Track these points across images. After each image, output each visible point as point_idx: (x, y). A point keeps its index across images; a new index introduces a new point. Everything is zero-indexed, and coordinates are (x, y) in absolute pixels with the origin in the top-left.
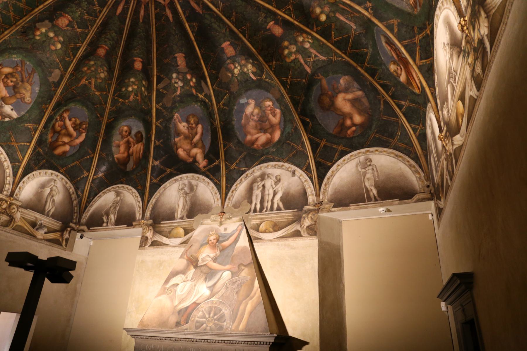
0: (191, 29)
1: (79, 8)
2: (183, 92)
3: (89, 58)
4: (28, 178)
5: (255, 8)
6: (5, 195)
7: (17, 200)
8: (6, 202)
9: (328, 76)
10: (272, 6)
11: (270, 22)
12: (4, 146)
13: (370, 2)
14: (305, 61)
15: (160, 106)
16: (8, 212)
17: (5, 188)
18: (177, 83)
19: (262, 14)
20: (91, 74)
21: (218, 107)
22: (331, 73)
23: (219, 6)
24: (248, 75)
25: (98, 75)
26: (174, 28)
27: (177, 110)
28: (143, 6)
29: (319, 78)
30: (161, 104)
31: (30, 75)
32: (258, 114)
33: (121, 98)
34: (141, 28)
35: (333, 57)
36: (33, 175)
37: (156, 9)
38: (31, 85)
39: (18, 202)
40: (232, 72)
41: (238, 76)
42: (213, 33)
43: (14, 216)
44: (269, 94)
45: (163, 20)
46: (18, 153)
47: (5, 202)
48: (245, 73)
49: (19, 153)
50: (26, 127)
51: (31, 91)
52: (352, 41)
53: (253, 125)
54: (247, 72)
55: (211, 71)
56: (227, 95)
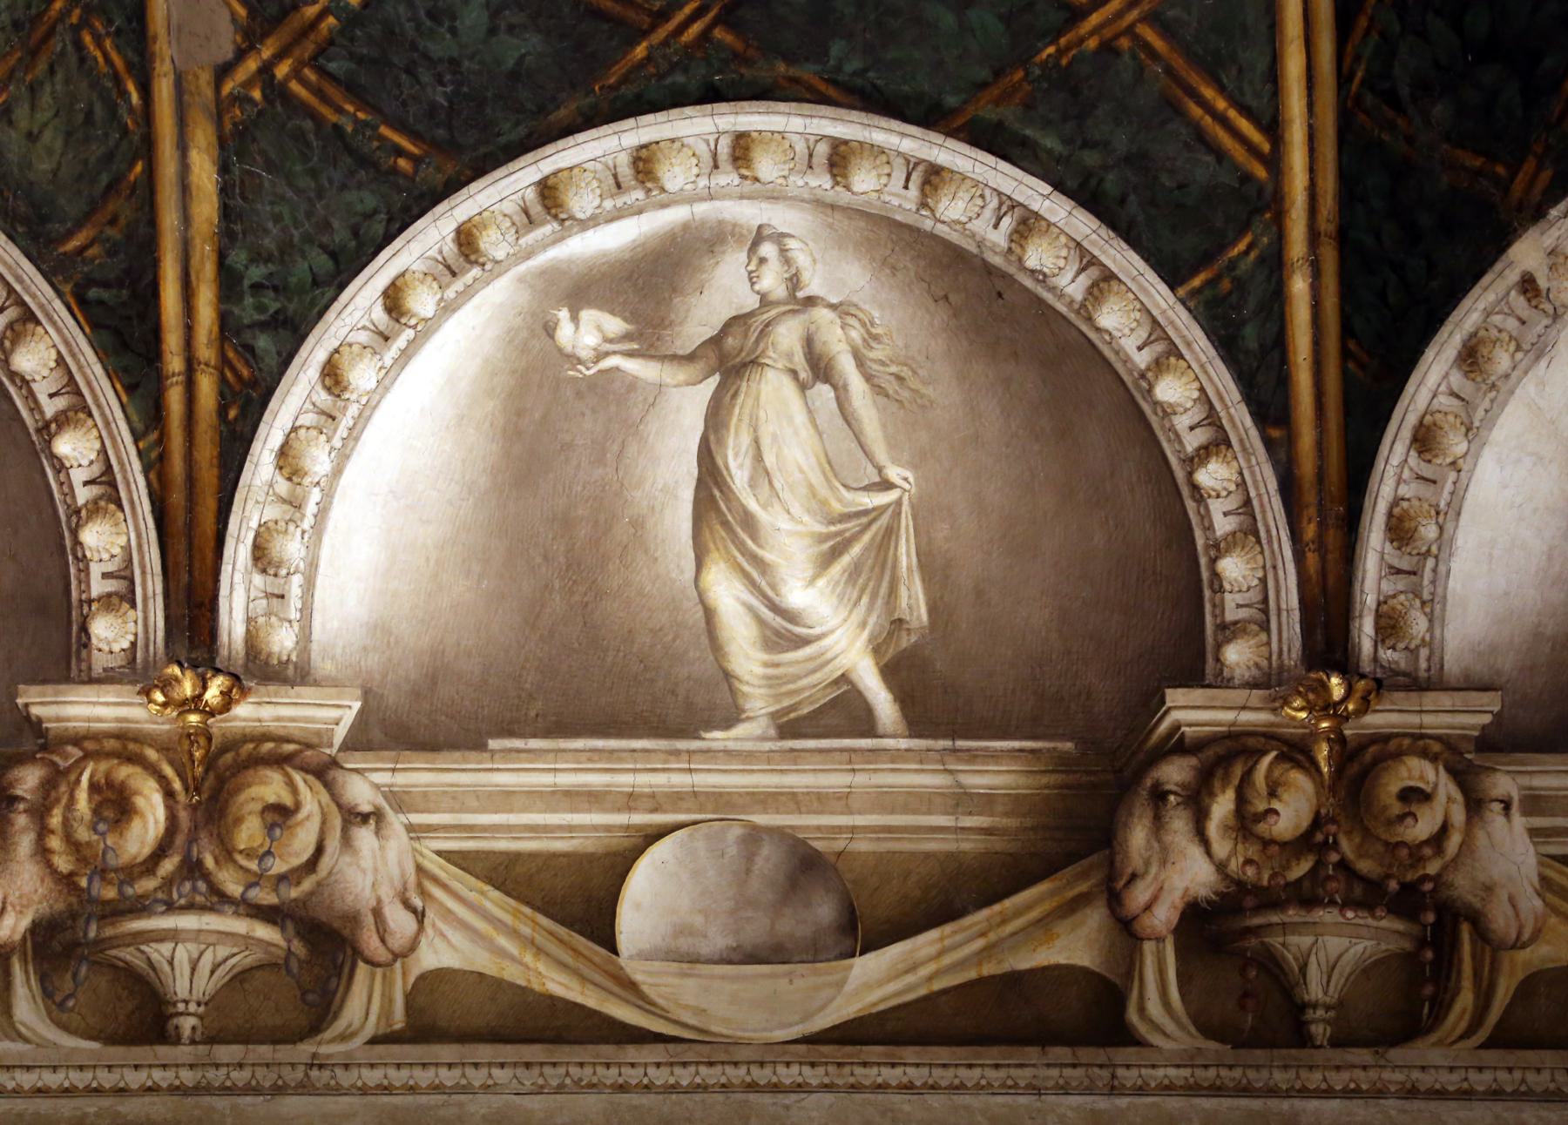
4: (1471, 357)
6: (1252, 685)
7: (1415, 684)
8: (1296, 751)
12: (1009, 113)
16: (1365, 866)
17: (1219, 607)
36: (1528, 285)
39: (1446, 700)
43: (1462, 886)
46: (1196, 111)
47: (1281, 758)
49: (1208, 93)
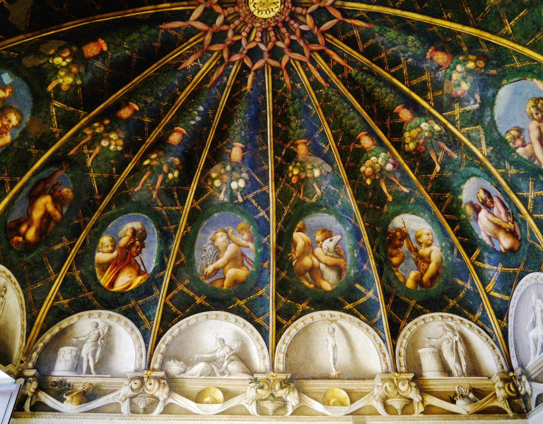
5: (160, 95)
9: (67, 174)
11: (137, 104)
13: (191, 229)
14: (84, 144)
22: (71, 175)
29: (64, 165)
35: (94, 173)
40: (58, 54)
52: (124, 193)
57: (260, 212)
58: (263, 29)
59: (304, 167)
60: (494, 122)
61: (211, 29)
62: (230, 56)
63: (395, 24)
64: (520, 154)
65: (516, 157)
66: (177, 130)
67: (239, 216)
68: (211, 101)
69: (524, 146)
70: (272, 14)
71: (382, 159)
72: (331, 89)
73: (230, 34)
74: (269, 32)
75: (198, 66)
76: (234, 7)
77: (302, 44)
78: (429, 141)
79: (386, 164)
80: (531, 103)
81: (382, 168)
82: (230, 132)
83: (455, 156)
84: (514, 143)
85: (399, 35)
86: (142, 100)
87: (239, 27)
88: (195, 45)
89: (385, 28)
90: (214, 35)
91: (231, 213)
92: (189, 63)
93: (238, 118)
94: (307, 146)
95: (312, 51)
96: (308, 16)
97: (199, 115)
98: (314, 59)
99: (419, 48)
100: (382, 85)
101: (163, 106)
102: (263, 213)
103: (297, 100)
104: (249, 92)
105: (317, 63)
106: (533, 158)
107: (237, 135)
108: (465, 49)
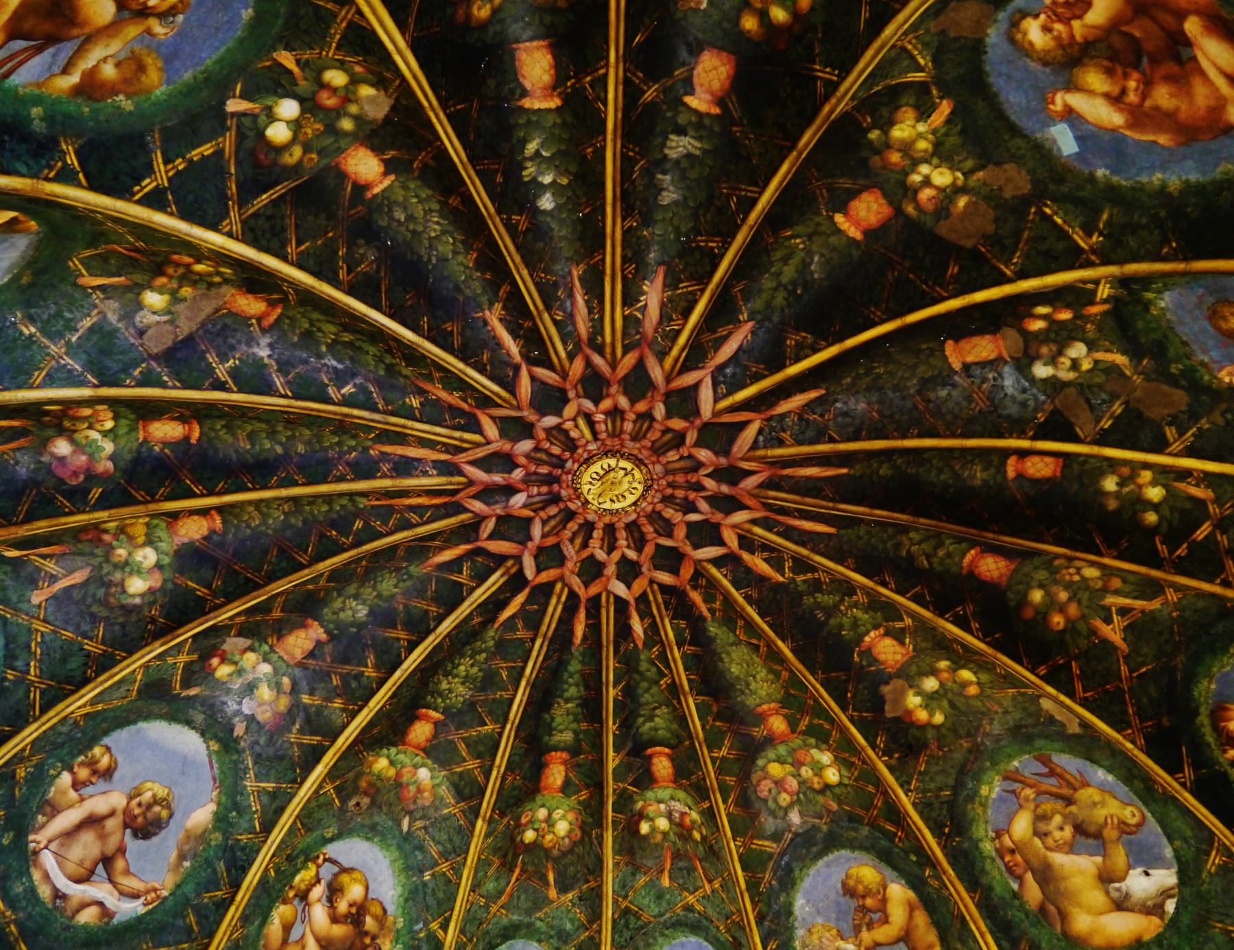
0: (807, 356)
1: (841, 611)
2: (1112, 343)
3: (1012, 604)
5: (659, 176)
10: (604, 148)
11: (696, 111)
15: (1181, 434)
18: (1075, 365)
19: (671, 148)
20: (1085, 602)
21: (1093, 257)
23: (690, 292)
24: (943, 130)
25: (1091, 584)
26: (848, 380)
27: (1203, 370)
28: (787, 471)
30: (1170, 432)
31: (1052, 773)
32: (1109, 72)
33: (1195, 531)
34: (875, 465)
37: (781, 443)
38: (1086, 784)
41: (959, 170)
42: (816, 276)
44: (989, 41)
45: (822, 416)
48: (937, 145)
50: (1217, 873)
51: (1107, 797)
53: (1171, 95)
54: (930, 136)
55: (949, 284)
56: (1048, 211)
57: (166, 163)
58: (577, 447)
59: (194, 284)
60: (134, 722)
61: (662, 390)
62: (589, 363)
63: (406, 606)
64: (58, 781)
65: (52, 772)
66: (552, 96)
67: (187, 76)
68: (541, 244)
69: (76, 785)
70: (586, 478)
71: (96, 441)
72: (360, 449)
73: (623, 402)
74: (564, 451)
75: (631, 305)
76: (654, 442)
77: (498, 478)
78: (98, 551)
79: (72, 441)
80: (161, 792)
81: (70, 434)
82: (430, 192)
83: (37, 598)
84: (82, 764)
85: (379, 596)
86: (692, 133)
87: (618, 423)
88: (671, 349)
89: (409, 583)
90: (651, 385)
91: (214, 57)
92: (653, 295)
93: (444, 232)
94: (250, 318)
95: (471, 483)
96: (532, 514)
97: (534, 180)
98: (451, 475)
99: (334, 613)
100: (293, 520)
101: (638, 162)
102: (162, 174)
103: (382, 372)
104: (483, 311)
105: (438, 475)
106: (48, 809)
107: (406, 198)
108: (306, 699)
